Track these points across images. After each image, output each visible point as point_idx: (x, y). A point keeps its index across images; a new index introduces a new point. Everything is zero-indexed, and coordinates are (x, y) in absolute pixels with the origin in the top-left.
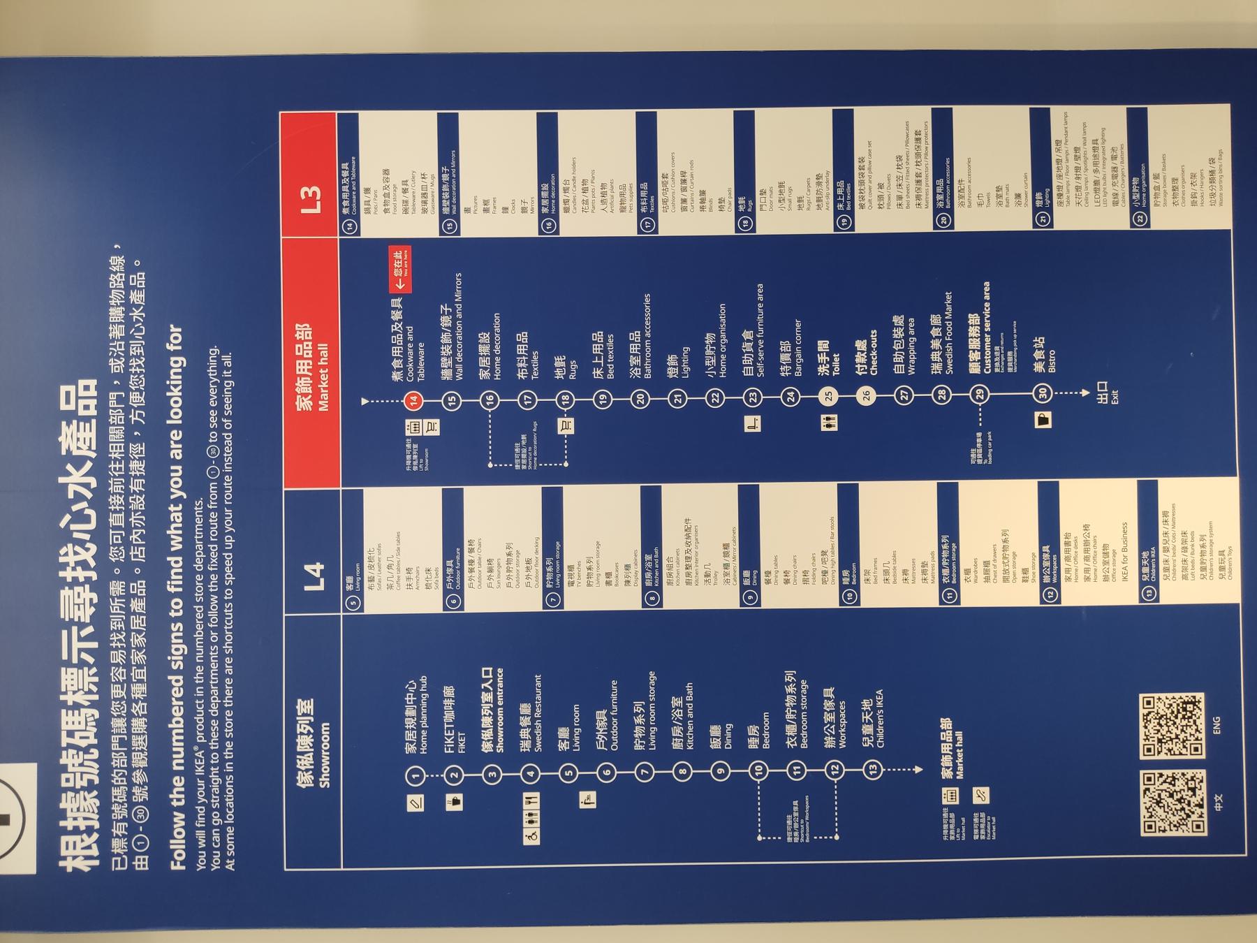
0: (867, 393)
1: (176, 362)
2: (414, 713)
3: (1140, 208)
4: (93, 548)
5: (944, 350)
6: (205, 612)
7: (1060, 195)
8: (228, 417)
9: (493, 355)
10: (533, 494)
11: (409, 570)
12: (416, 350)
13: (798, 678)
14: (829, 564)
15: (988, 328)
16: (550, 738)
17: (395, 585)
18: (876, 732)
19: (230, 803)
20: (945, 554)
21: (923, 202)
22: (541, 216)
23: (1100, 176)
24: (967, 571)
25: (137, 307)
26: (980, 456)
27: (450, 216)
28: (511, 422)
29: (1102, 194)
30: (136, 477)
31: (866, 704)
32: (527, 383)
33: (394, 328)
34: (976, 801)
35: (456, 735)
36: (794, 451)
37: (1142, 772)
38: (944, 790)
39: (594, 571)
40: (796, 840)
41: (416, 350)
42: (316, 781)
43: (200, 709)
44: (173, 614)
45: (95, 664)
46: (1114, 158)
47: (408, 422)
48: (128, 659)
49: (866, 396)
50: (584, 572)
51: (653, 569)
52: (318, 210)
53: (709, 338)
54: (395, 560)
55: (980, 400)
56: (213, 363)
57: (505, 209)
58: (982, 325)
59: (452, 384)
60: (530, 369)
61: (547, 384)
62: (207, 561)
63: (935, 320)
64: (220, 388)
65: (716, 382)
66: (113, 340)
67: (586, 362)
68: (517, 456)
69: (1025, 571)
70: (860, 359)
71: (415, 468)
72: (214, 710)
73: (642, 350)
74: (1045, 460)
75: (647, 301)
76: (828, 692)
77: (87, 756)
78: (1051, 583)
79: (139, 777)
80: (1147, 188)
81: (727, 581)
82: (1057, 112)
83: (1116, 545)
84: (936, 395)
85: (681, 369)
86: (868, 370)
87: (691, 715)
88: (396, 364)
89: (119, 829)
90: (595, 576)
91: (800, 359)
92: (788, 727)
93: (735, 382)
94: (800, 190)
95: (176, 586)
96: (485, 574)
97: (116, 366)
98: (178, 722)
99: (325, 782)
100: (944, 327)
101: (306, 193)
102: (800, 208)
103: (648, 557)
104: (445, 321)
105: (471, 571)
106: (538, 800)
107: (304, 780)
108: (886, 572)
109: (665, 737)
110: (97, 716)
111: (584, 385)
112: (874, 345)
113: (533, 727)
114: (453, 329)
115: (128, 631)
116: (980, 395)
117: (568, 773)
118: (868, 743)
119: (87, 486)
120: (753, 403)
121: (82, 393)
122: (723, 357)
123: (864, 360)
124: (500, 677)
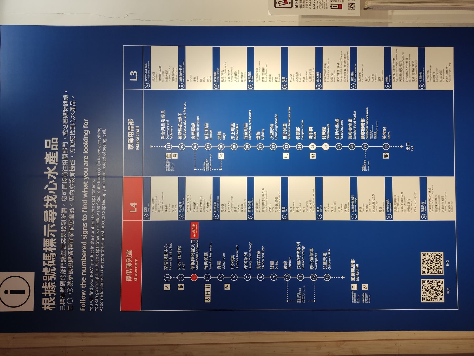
0: (326, 146)
1: (86, 132)
2: (167, 255)
3: (422, 82)
4: (56, 197)
5: (353, 131)
6: (95, 219)
7: (394, 78)
8: (104, 152)
9: (196, 131)
10: (209, 180)
11: (166, 206)
12: (170, 128)
13: (301, 245)
14: (312, 205)
15: (367, 124)
16: (215, 265)
17: (161, 211)
18: (328, 264)
19: (102, 287)
20: (353, 202)
21: (346, 80)
22: (214, 83)
23: (408, 71)
24: (360, 208)
25: (73, 112)
27: (182, 82)
28: (202, 154)
29: (409, 77)
30: (72, 172)
31: (324, 254)
32: (208, 141)
33: (162, 121)
34: (363, 289)
35: (182, 263)
36: (300, 166)
37: (422, 280)
38: (352, 285)
39: (231, 207)
40: (300, 302)
41: (170, 128)
42: (132, 279)
43: (92, 254)
44: (84, 220)
45: (55, 238)
46: (413, 65)
47: (166, 154)
48: (67, 236)
49: (326, 147)
50: (227, 207)
51: (251, 206)
52: (136, 80)
53: (272, 126)
54: (161, 202)
55: (365, 149)
56: (99, 133)
57: (201, 80)
59: (182, 141)
60: (209, 136)
61: (215, 141)
62: (96, 201)
63: (350, 120)
64: (102, 141)
65: (274, 141)
66: (64, 124)
67: (229, 133)
69: (380, 208)
70: (323, 134)
71: (169, 170)
72: (97, 254)
73: (248, 130)
74: (387, 169)
75: (250, 113)
76: (311, 250)
77: (52, 270)
78: (389, 213)
79: (70, 278)
80: (425, 76)
81: (277, 211)
82: (393, 49)
83: (412, 199)
84: (350, 147)
85: (261, 137)
86: (326, 138)
87: (263, 257)
88: (163, 133)
89: (62, 296)
90: (231, 208)
91: (303, 133)
92: (297, 262)
93: (280, 141)
94: (304, 75)
95: (85, 210)
96: (193, 207)
97: (65, 133)
98: (84, 258)
99: (136, 280)
101: (132, 74)
102: (304, 81)
103: (249, 202)
104: (180, 119)
105: (188, 206)
106: (210, 287)
107: (128, 279)
108: (332, 208)
109: (254, 265)
110: (56, 256)
111: (228, 141)
112: (328, 129)
113: (208, 261)
114: (183, 121)
115: (68, 226)
116: (365, 147)
117: (220, 277)
118: (325, 268)
119: (54, 175)
120: (286, 149)
121: (53, 142)
122: (276, 133)
123: (325, 134)
124: (197, 243)
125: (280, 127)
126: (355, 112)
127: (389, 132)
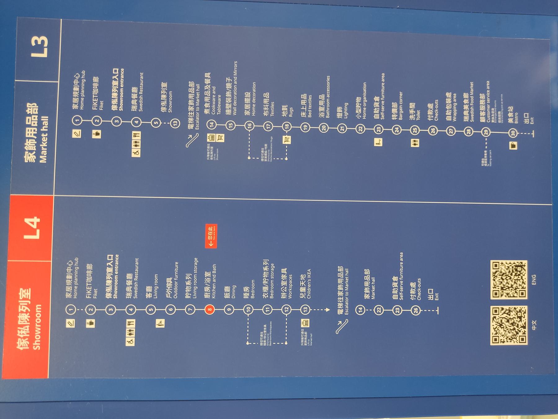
5: (470, 110)
9: (251, 103)
26: (486, 162)
32: (268, 118)
53: (358, 99)
55: (486, 135)
58: (486, 99)
61: (278, 119)
63: (466, 95)
65: (361, 121)
67: (298, 108)
68: (262, 155)
70: (430, 112)
71: (211, 159)
75: (328, 79)
85: (343, 114)
91: (401, 111)
93: (370, 121)
100: (470, 99)
104: (229, 86)
111: (296, 120)
114: (232, 89)
116: (486, 132)
122: (365, 109)
123: (431, 113)
125: (371, 102)
126: (472, 84)
127: (516, 114)
